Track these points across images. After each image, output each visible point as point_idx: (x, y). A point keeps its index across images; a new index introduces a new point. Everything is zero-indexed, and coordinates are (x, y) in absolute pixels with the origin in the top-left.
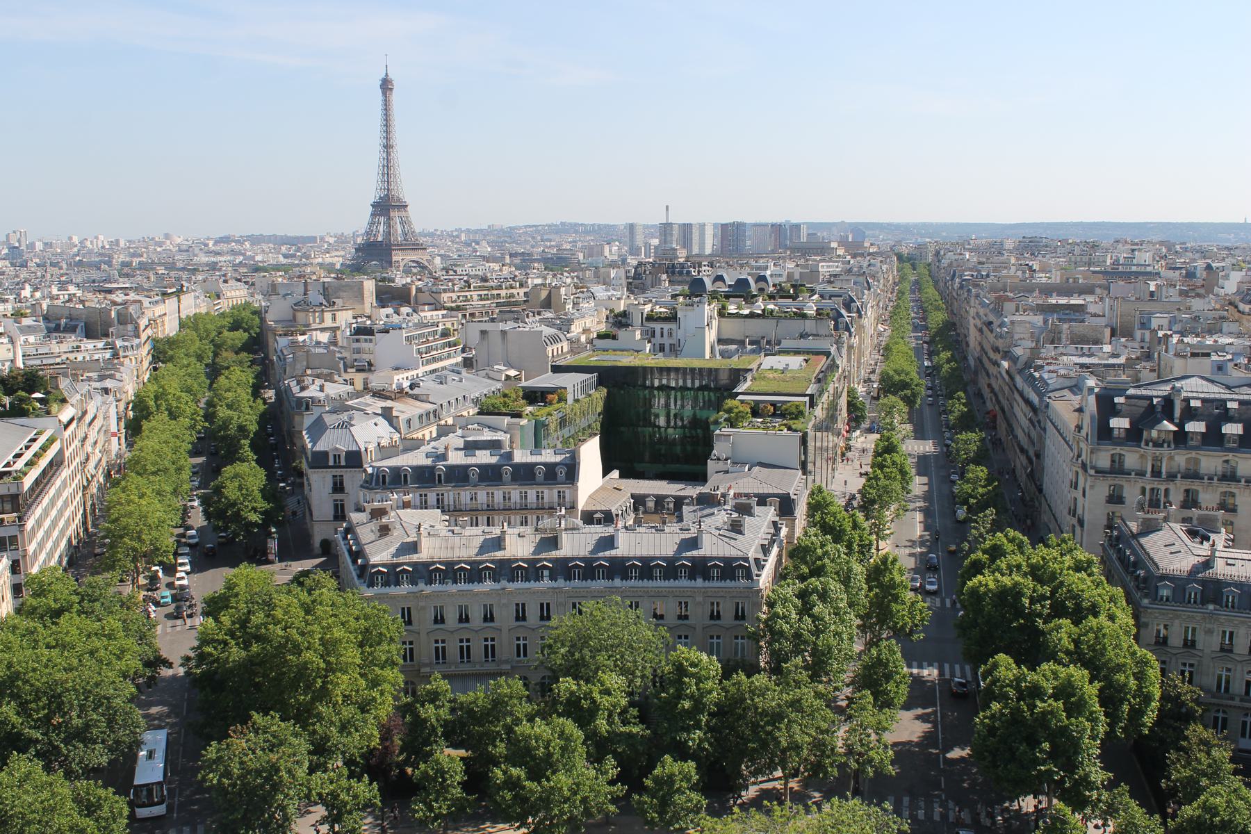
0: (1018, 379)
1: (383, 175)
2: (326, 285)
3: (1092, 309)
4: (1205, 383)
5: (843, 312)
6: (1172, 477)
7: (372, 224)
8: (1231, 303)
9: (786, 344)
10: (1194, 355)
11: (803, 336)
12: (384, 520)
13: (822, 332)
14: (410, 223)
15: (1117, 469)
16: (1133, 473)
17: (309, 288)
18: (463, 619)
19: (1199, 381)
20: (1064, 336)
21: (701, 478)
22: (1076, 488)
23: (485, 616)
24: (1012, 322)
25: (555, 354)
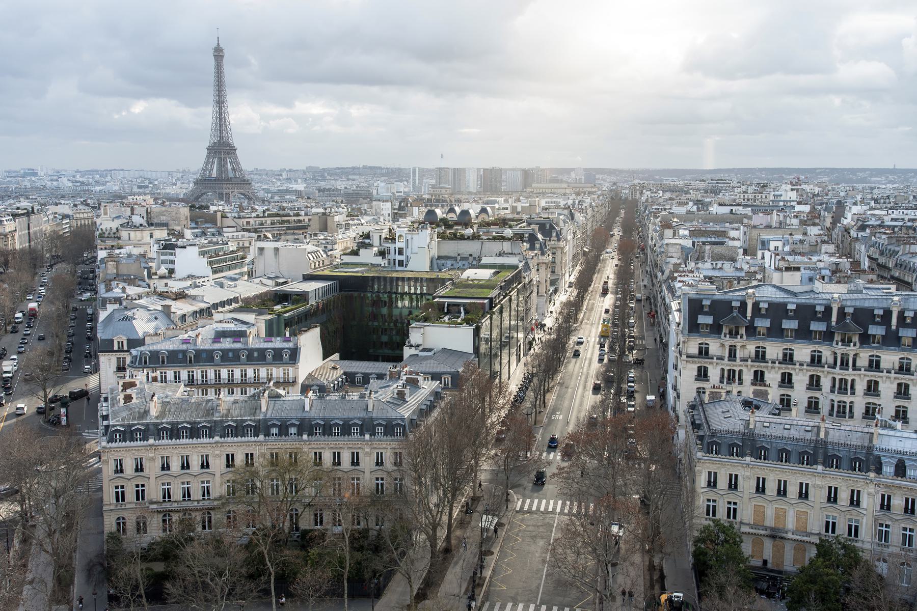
0: (664, 287)
1: (216, 125)
2: (149, 210)
3: (733, 234)
4: (774, 289)
5: (540, 236)
6: (744, 360)
7: (207, 163)
8: (846, 230)
9: (485, 260)
10: (788, 269)
11: (500, 255)
12: (129, 391)
13: (515, 251)
14: (238, 164)
15: (704, 352)
16: (715, 358)
17: (135, 212)
18: (185, 466)
19: (770, 288)
20: (706, 255)
21: (399, 359)
22: (676, 369)
23: (203, 464)
24: (667, 244)
25: (317, 266)
